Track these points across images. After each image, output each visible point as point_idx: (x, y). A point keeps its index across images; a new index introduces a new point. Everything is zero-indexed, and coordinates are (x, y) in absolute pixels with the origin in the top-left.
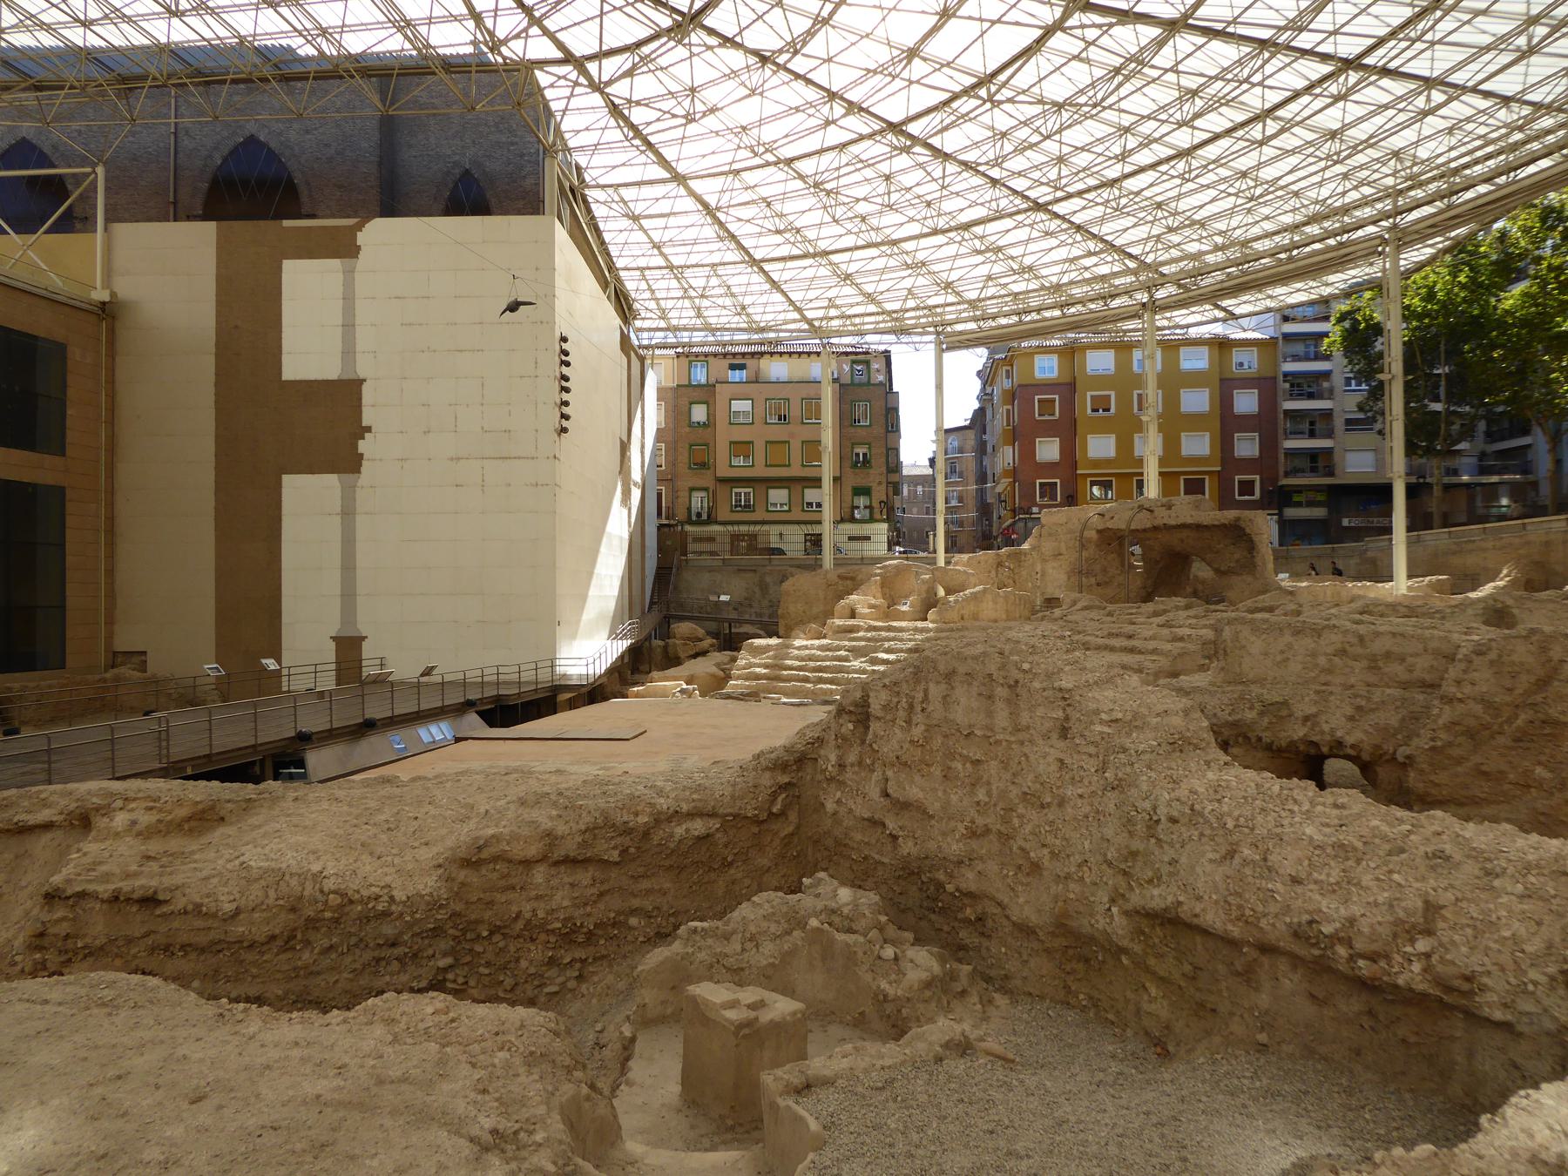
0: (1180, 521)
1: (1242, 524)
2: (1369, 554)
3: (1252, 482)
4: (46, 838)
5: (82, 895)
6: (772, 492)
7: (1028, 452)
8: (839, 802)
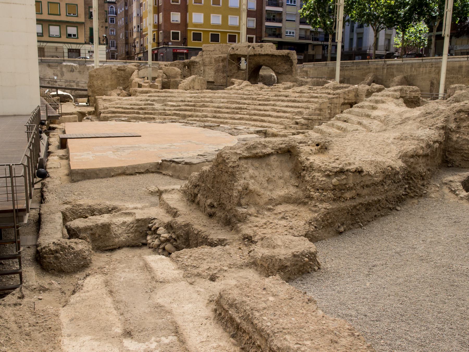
0: (266, 52)
1: (290, 55)
2: (304, 69)
3: (253, 38)
4: (272, 158)
5: (347, 170)
6: (51, 27)
7: (167, 18)
8: (458, 137)
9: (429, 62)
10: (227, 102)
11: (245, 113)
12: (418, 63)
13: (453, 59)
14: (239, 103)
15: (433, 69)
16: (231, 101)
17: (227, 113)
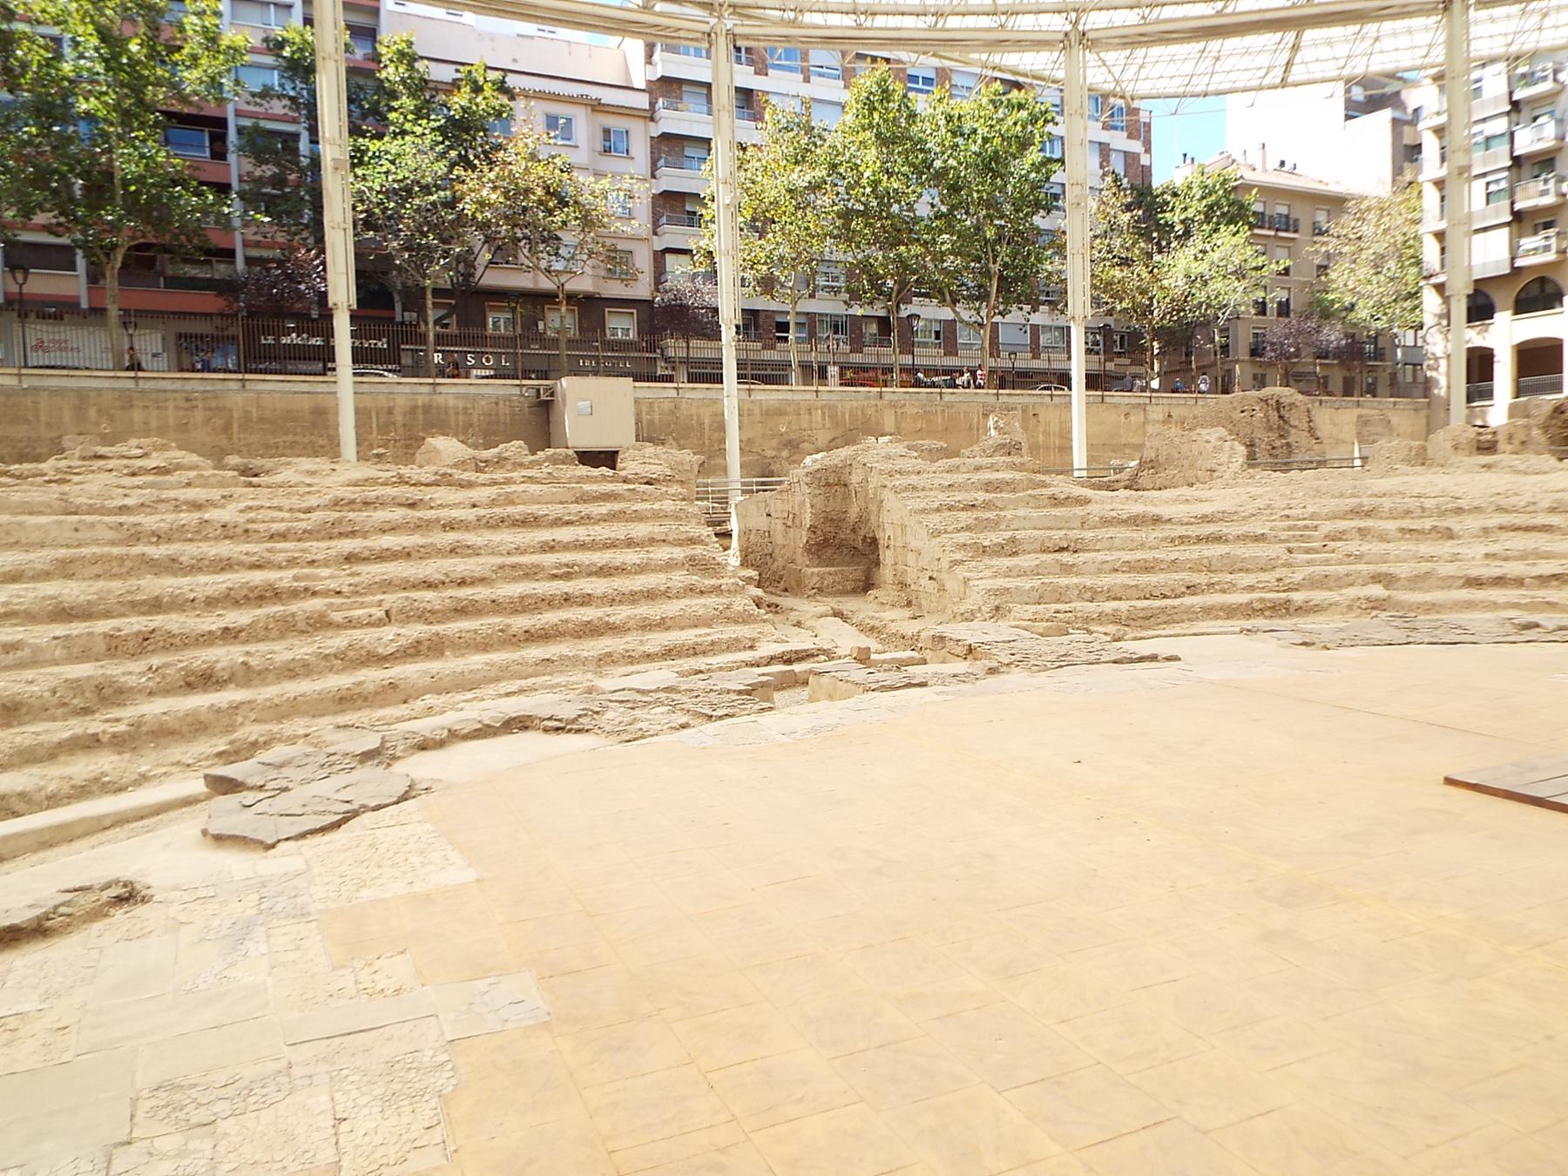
9: (174, 391)
10: (64, 569)
11: (380, 614)
12: (114, 390)
13: (287, 387)
14: (171, 566)
15: (199, 415)
16: (96, 560)
17: (229, 635)
